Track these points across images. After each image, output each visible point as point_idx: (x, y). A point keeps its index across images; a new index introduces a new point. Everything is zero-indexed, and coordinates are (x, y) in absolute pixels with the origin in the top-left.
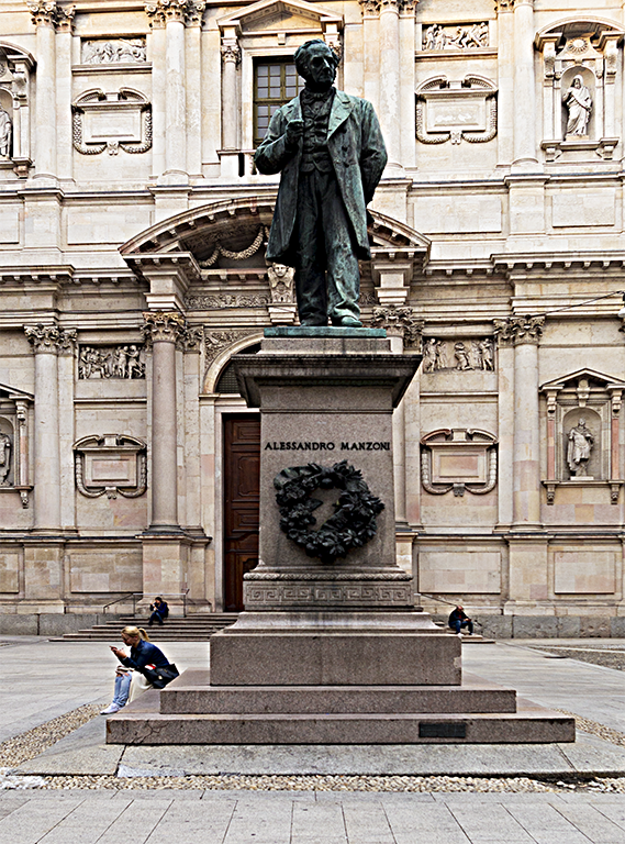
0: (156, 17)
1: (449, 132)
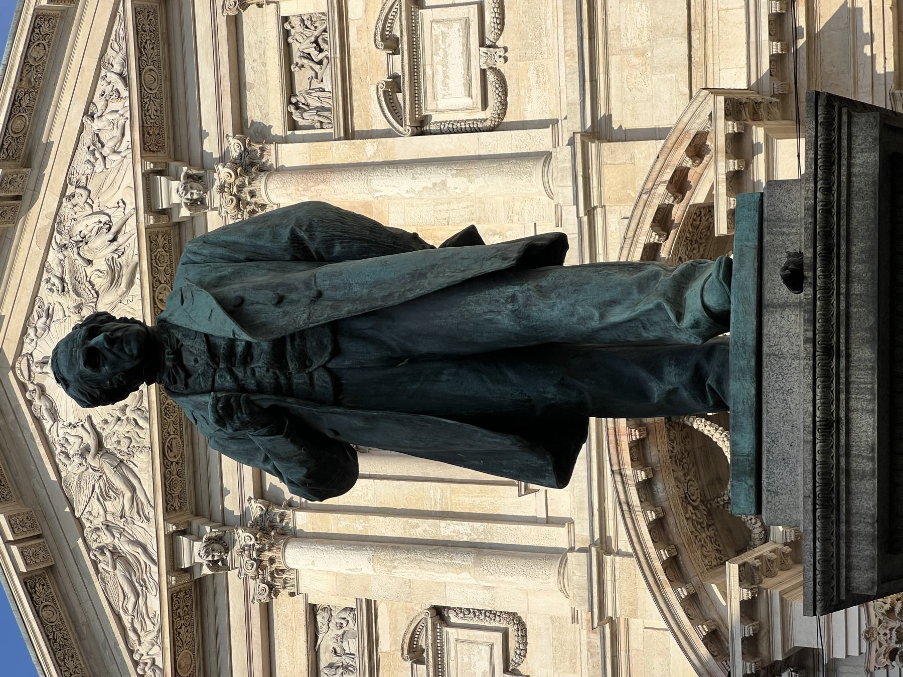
0: (279, 584)
1: (483, 72)
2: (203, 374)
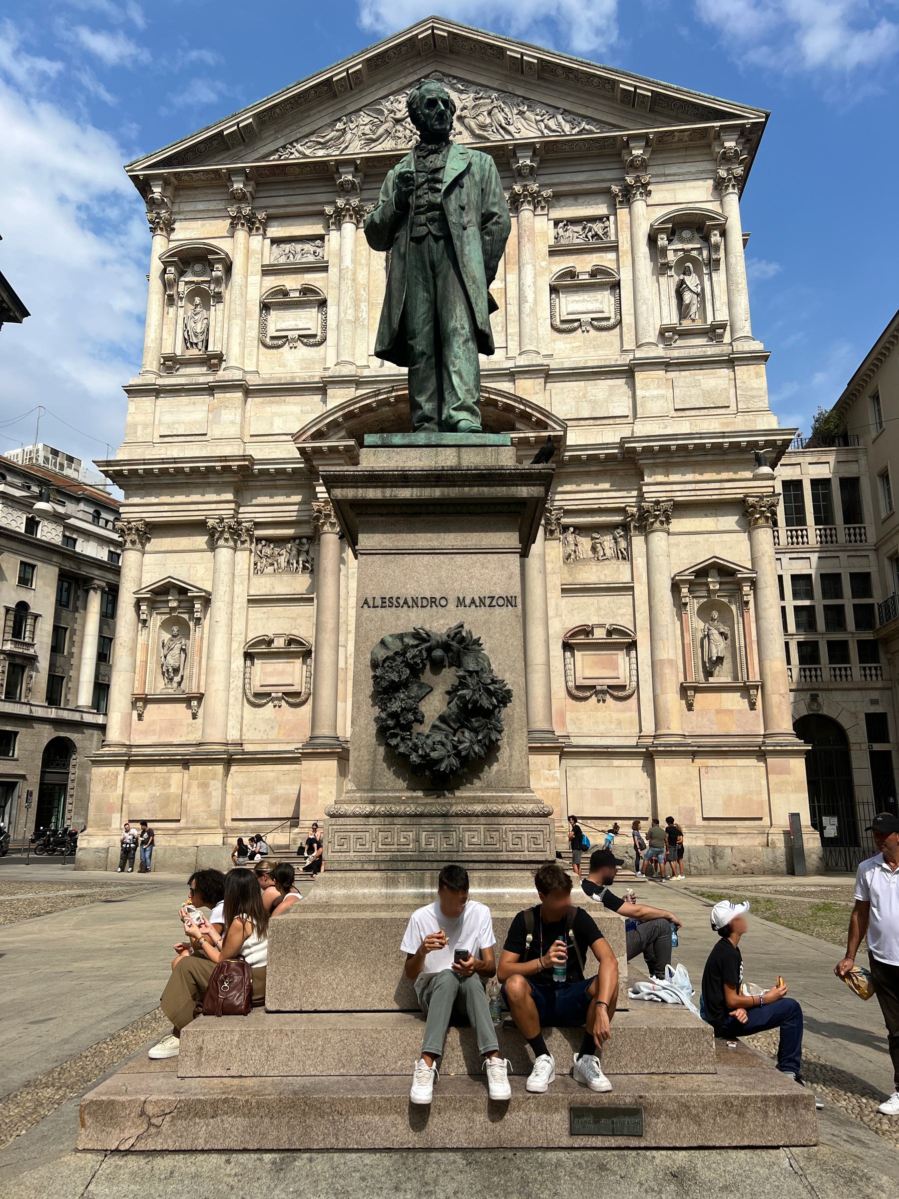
1: (579, 320)
2: (425, 166)
